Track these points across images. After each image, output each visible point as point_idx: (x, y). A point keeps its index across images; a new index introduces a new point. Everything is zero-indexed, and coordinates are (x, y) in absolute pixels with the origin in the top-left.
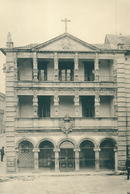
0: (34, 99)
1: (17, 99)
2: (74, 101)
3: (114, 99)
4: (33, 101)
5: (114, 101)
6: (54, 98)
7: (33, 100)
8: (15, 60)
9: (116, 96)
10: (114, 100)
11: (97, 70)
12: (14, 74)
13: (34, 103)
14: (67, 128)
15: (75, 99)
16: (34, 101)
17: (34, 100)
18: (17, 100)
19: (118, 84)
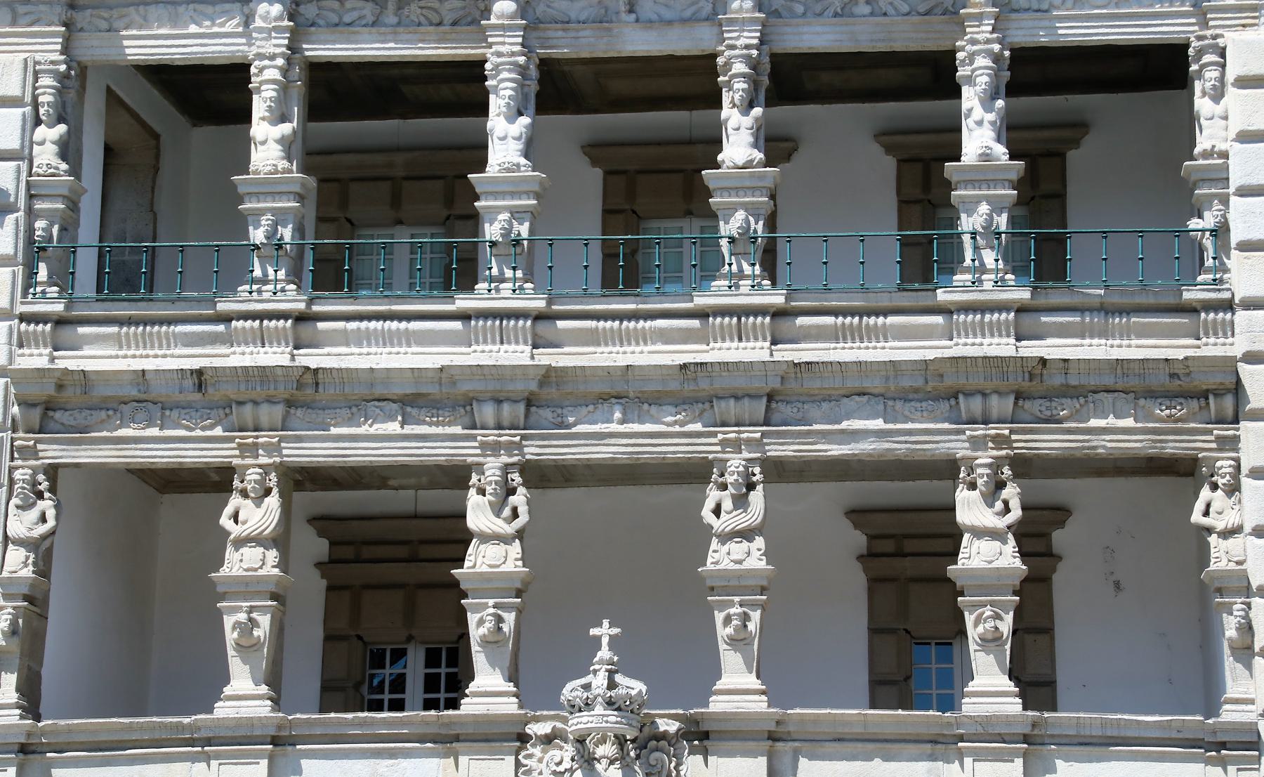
0: (235, 501)
1: (34, 514)
2: (707, 514)
3: (1205, 493)
4: (225, 521)
5: (1197, 517)
6: (472, 492)
7: (229, 510)
8: (46, 81)
9: (1225, 465)
10: (1199, 506)
11: (986, 156)
12: (30, 230)
13: (230, 553)
15: (713, 495)
16: (235, 530)
17: (235, 517)
19: (1241, 316)
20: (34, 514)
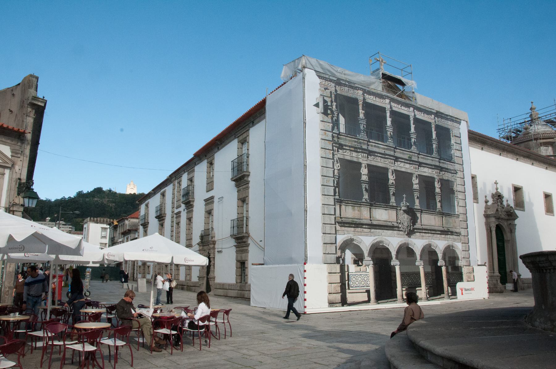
14: (406, 224)
18: (337, 166)
20: (337, 165)
